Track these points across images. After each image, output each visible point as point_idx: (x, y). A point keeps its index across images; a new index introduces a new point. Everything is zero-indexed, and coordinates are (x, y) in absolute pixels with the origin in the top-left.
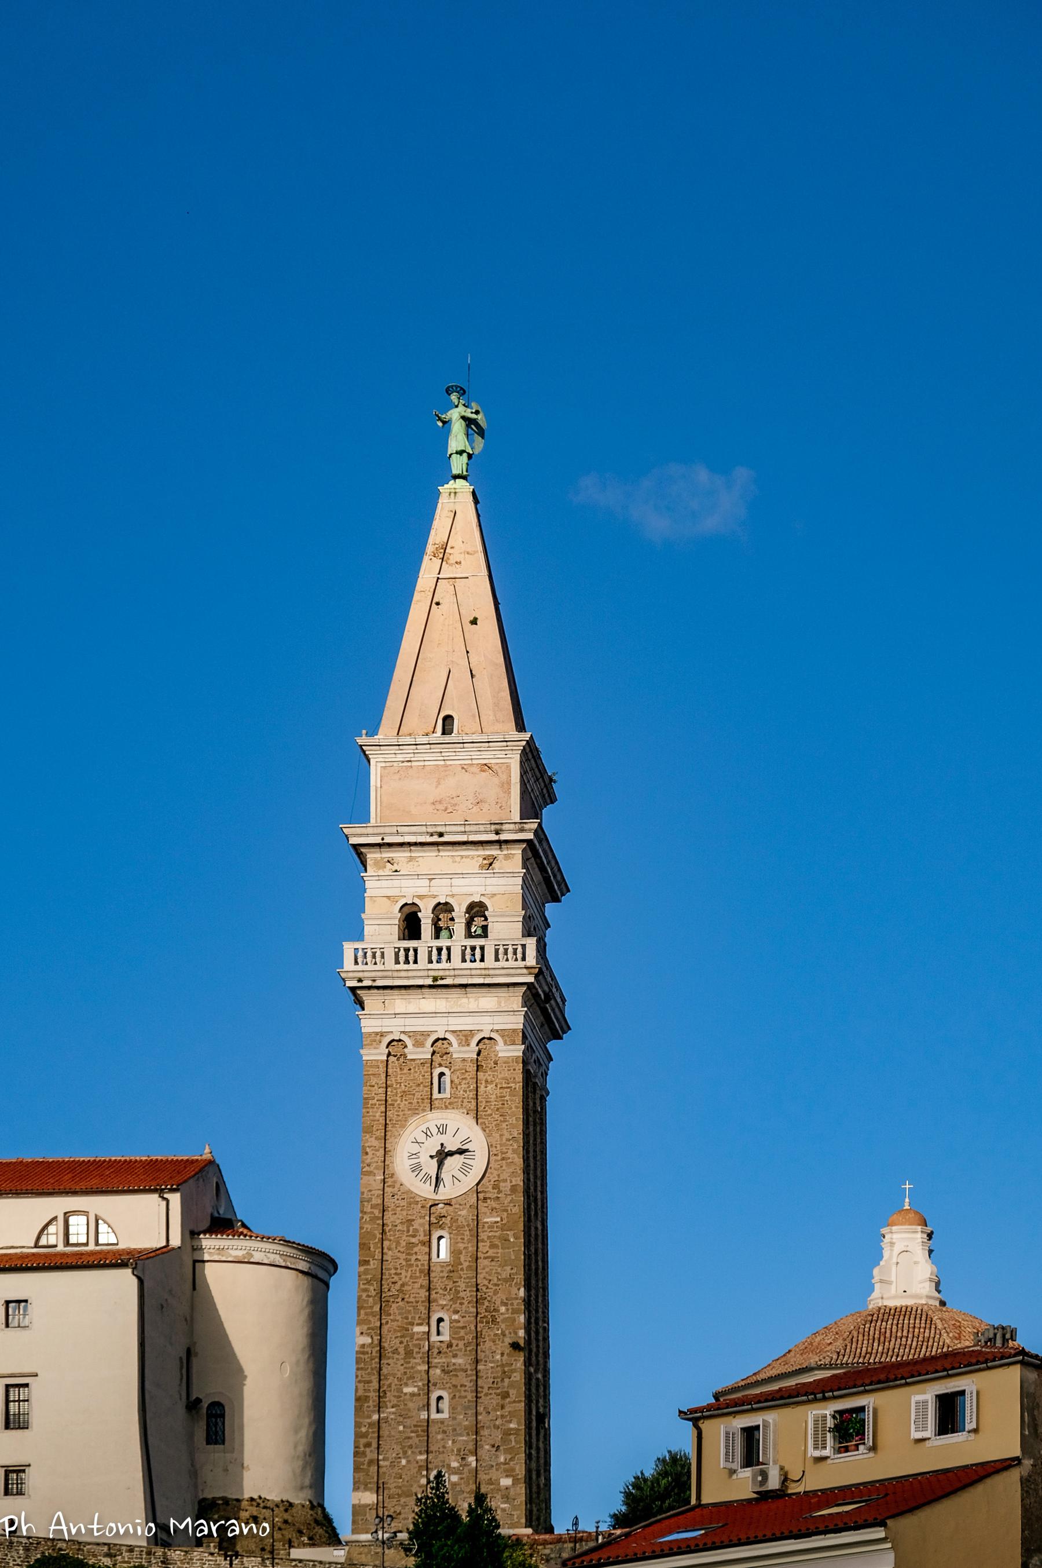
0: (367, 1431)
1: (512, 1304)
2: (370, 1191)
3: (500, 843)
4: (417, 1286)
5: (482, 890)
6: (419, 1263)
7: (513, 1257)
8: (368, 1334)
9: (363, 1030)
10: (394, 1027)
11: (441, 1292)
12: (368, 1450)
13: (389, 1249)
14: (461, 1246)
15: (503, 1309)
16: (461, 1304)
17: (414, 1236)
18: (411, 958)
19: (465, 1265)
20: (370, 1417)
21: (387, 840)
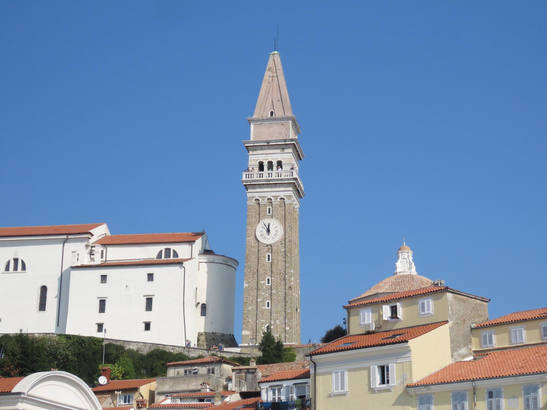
0: (247, 313)
1: (289, 275)
2: (249, 242)
3: (286, 144)
4: (262, 269)
5: (280, 157)
6: (262, 263)
7: (289, 261)
8: (247, 284)
9: (248, 196)
10: (257, 196)
11: (269, 271)
12: (247, 318)
13: (254, 258)
14: (275, 257)
15: (286, 276)
16: (274, 275)
17: (261, 255)
18: (261, 176)
19: (275, 263)
20: (248, 308)
21: (255, 144)
